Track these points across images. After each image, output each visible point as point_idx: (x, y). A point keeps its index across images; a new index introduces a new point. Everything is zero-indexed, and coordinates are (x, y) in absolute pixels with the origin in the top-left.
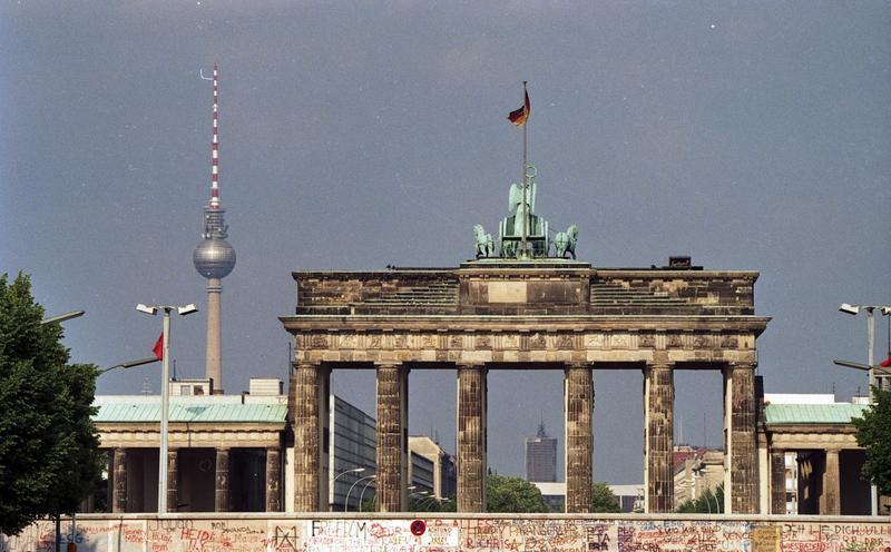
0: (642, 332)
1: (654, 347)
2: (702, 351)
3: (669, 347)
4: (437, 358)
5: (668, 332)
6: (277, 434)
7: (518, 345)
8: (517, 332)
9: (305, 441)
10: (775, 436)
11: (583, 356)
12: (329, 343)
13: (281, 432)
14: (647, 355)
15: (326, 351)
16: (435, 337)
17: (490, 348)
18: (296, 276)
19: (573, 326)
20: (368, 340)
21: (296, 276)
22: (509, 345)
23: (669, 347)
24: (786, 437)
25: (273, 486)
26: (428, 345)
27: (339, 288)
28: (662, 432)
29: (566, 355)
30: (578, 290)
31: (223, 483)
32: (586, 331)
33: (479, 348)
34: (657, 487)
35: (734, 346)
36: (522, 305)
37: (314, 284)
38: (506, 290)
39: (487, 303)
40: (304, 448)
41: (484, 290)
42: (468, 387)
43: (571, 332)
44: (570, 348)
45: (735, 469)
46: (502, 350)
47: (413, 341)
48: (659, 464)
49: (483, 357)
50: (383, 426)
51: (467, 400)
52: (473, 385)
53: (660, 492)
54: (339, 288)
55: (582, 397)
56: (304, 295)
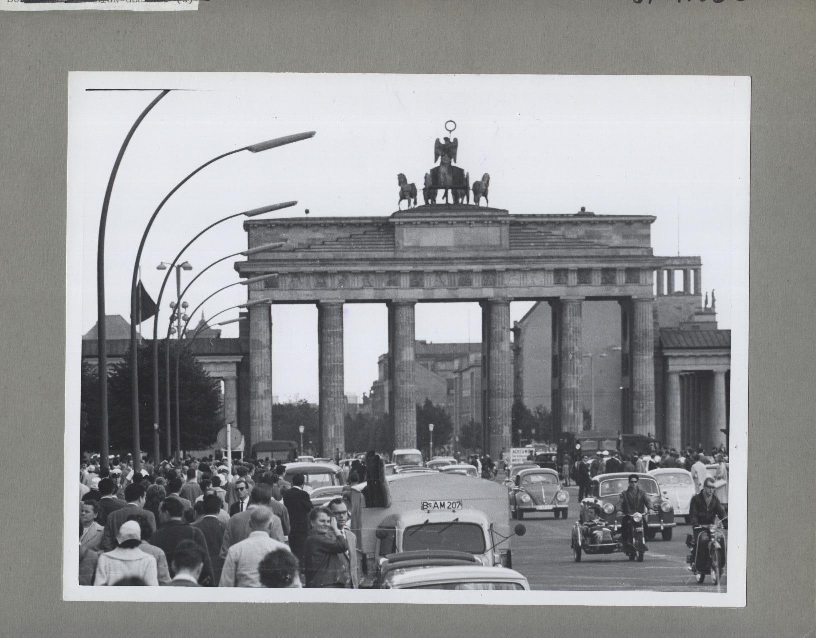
0: (557, 272)
5: (580, 271)
6: (234, 367)
7: (447, 283)
8: (447, 272)
10: (671, 362)
13: (238, 363)
16: (372, 277)
19: (498, 267)
20: (313, 281)
29: (489, 293)
35: (637, 281)
43: (494, 272)
44: (494, 285)
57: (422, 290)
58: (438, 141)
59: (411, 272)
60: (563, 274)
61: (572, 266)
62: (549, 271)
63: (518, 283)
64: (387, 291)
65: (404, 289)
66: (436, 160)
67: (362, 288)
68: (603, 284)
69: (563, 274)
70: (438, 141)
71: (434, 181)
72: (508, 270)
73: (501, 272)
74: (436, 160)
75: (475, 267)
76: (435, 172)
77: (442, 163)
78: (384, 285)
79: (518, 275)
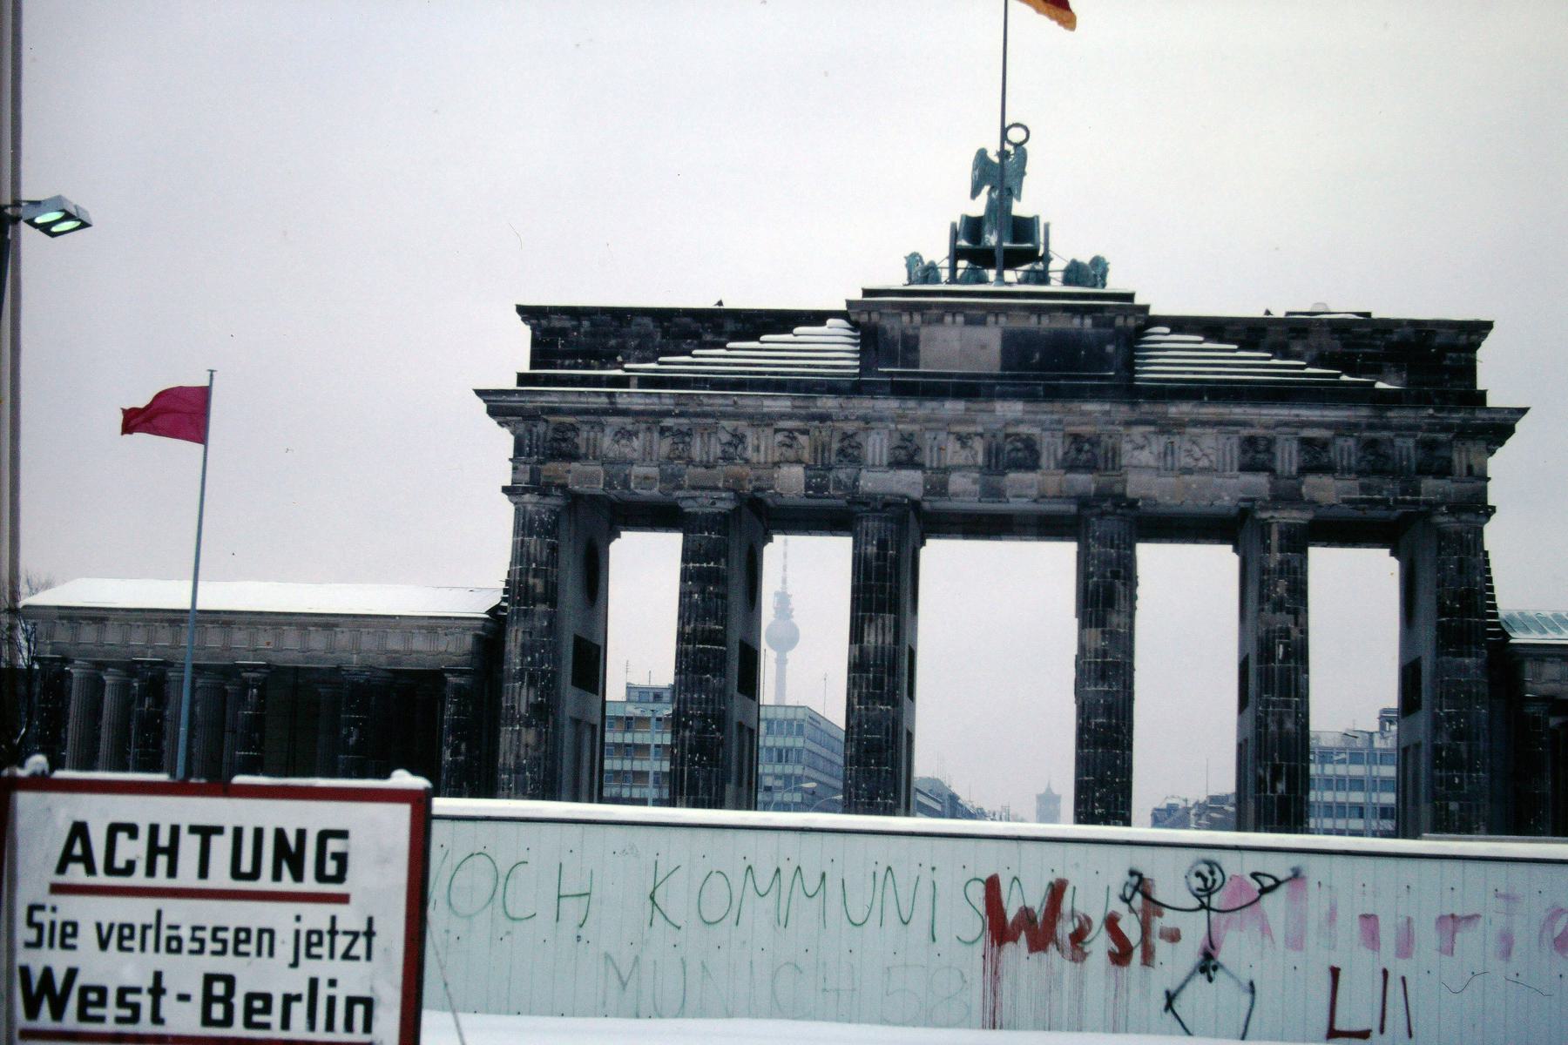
1: (1272, 471)
2: (1375, 480)
3: (1304, 470)
4: (808, 487)
5: (1306, 443)
6: (468, 641)
7: (980, 459)
9: (524, 655)
10: (1529, 668)
11: (1118, 489)
12: (583, 450)
15: (575, 465)
17: (919, 466)
18: (526, 313)
21: (528, 313)
23: (1304, 470)
24: (1552, 670)
25: (455, 752)
26: (790, 454)
27: (613, 342)
28: (1286, 653)
29: (1084, 482)
30: (1110, 348)
31: (352, 740)
33: (896, 464)
34: (1276, 777)
35: (1444, 471)
36: (990, 376)
37: (563, 332)
38: (957, 345)
40: (521, 672)
41: (910, 345)
42: (872, 550)
44: (1090, 467)
45: (1444, 740)
46: (947, 470)
47: (757, 449)
48: (1281, 724)
49: (908, 483)
50: (688, 629)
51: (867, 577)
52: (882, 545)
53: (1281, 787)
54: (613, 342)
55: (1116, 575)
56: (542, 352)
57: (916, 476)
58: (982, 155)
63: (1152, 463)
64: (832, 475)
66: (975, 193)
67: (777, 464)
70: (982, 155)
71: (972, 245)
74: (975, 193)
76: (973, 227)
77: (991, 207)
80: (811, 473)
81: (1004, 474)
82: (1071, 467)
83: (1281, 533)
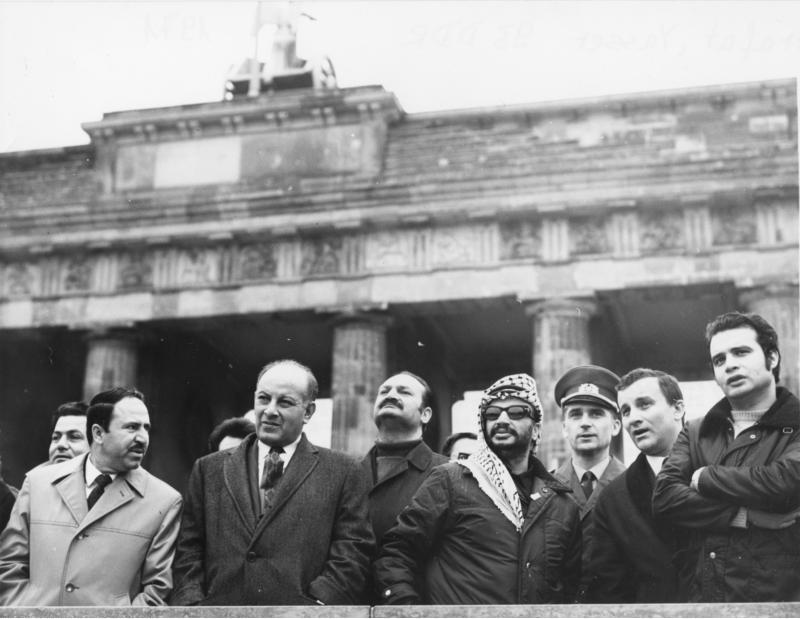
3: (573, 258)
7: (213, 275)
14: (522, 282)
22: (191, 279)
32: (369, 228)
35: (748, 241)
36: (229, 185)
39: (149, 188)
46: (174, 291)
49: (136, 309)
57: (146, 299)
59: (118, 249)
60: (526, 230)
61: (544, 199)
62: (485, 221)
64: (61, 304)
65: (99, 295)
68: (645, 254)
69: (526, 230)
72: (369, 228)
73: (352, 232)
75: (278, 222)
78: (58, 287)
79: (406, 242)
80: (39, 305)
81: (237, 287)
82: (309, 278)
83: (552, 328)
